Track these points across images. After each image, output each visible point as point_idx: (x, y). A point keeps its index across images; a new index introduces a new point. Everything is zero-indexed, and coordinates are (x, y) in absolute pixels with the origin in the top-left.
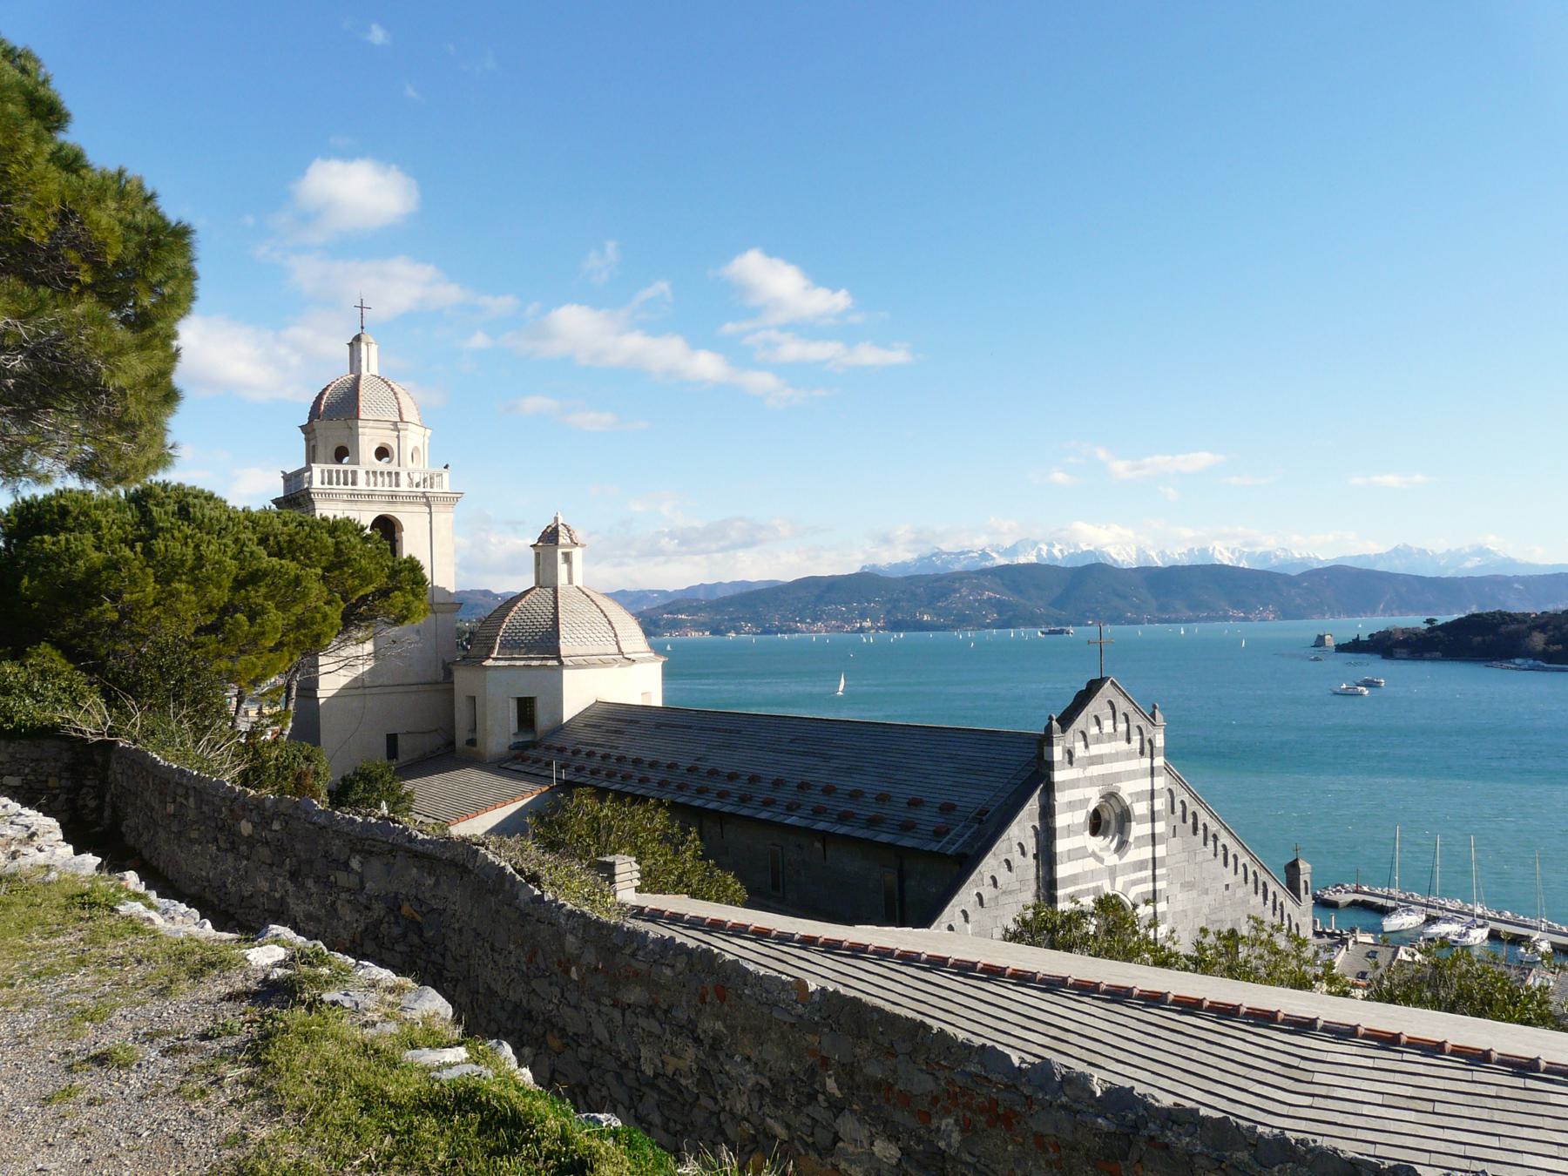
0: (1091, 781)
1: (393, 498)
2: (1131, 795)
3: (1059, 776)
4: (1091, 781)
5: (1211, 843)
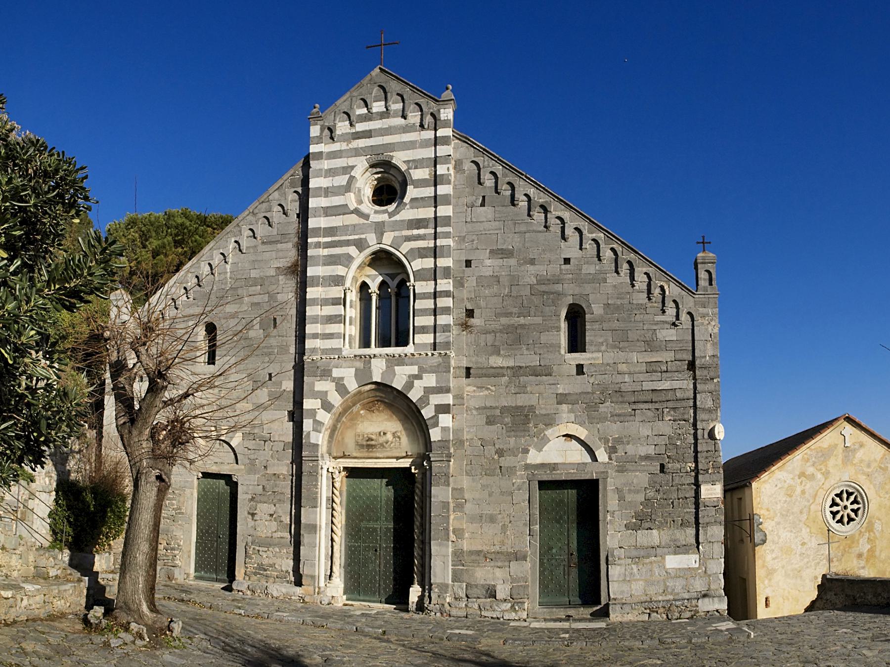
0: (357, 152)
4: (357, 152)
5: (538, 216)
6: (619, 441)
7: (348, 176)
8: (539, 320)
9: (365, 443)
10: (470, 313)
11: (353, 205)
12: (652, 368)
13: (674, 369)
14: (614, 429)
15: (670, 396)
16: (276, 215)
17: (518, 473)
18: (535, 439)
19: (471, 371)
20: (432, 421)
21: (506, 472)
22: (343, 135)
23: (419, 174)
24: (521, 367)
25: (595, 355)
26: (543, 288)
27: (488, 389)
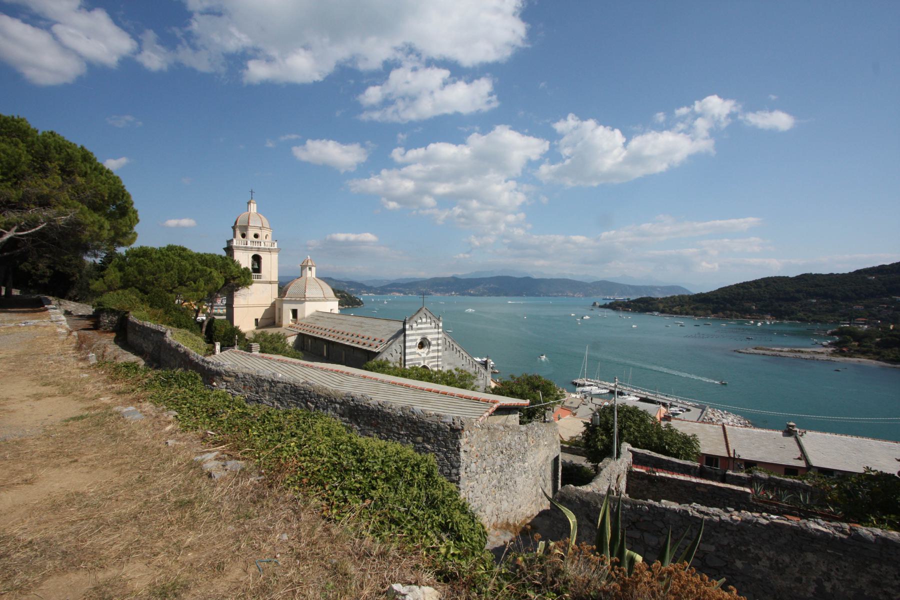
0: (418, 334)
1: (259, 250)
3: (407, 332)
4: (418, 334)
16: (394, 353)
23: (434, 342)
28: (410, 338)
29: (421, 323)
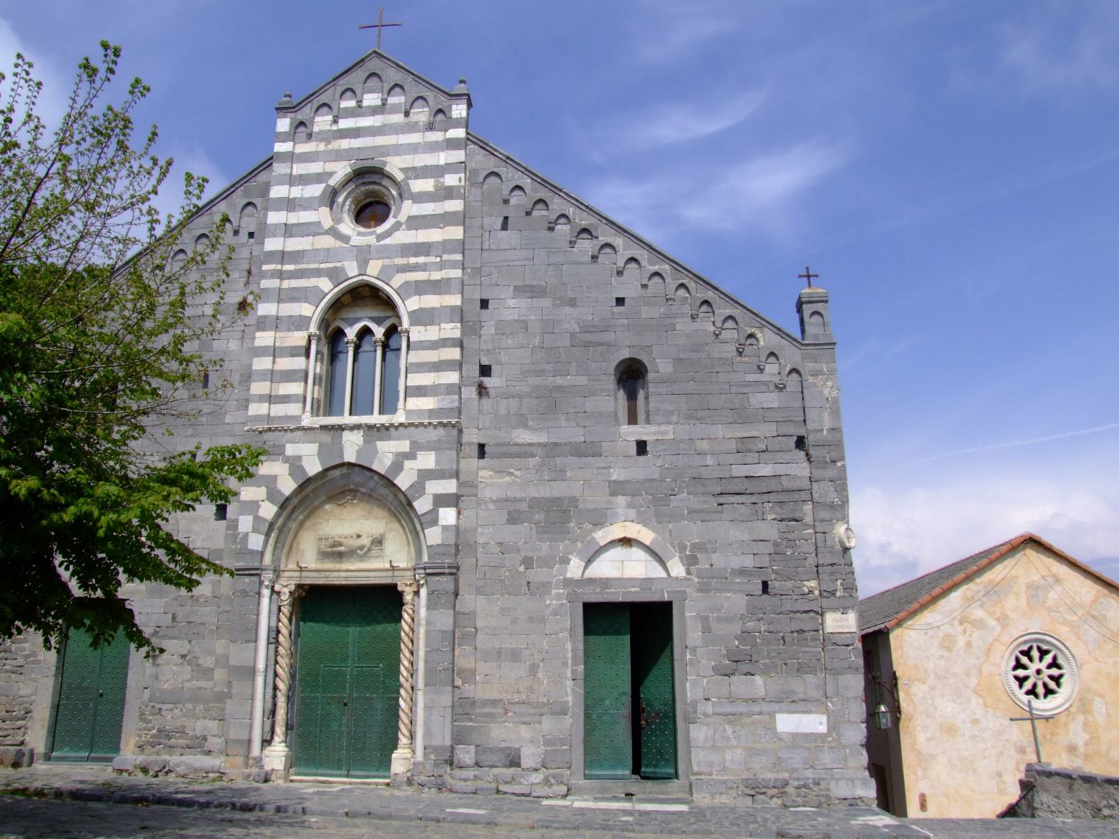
0: (338, 156)
2: (404, 170)
6: (698, 547)
7: (324, 185)
8: (582, 380)
9: (329, 550)
10: (485, 371)
11: (327, 223)
12: (744, 447)
13: (777, 448)
14: (694, 531)
15: (773, 485)
17: (554, 591)
18: (579, 545)
19: (487, 449)
20: (429, 517)
21: (537, 590)
22: (320, 133)
24: (556, 444)
25: (663, 428)
26: (589, 337)
27: (511, 474)
28: (298, 169)
29: (359, 111)
